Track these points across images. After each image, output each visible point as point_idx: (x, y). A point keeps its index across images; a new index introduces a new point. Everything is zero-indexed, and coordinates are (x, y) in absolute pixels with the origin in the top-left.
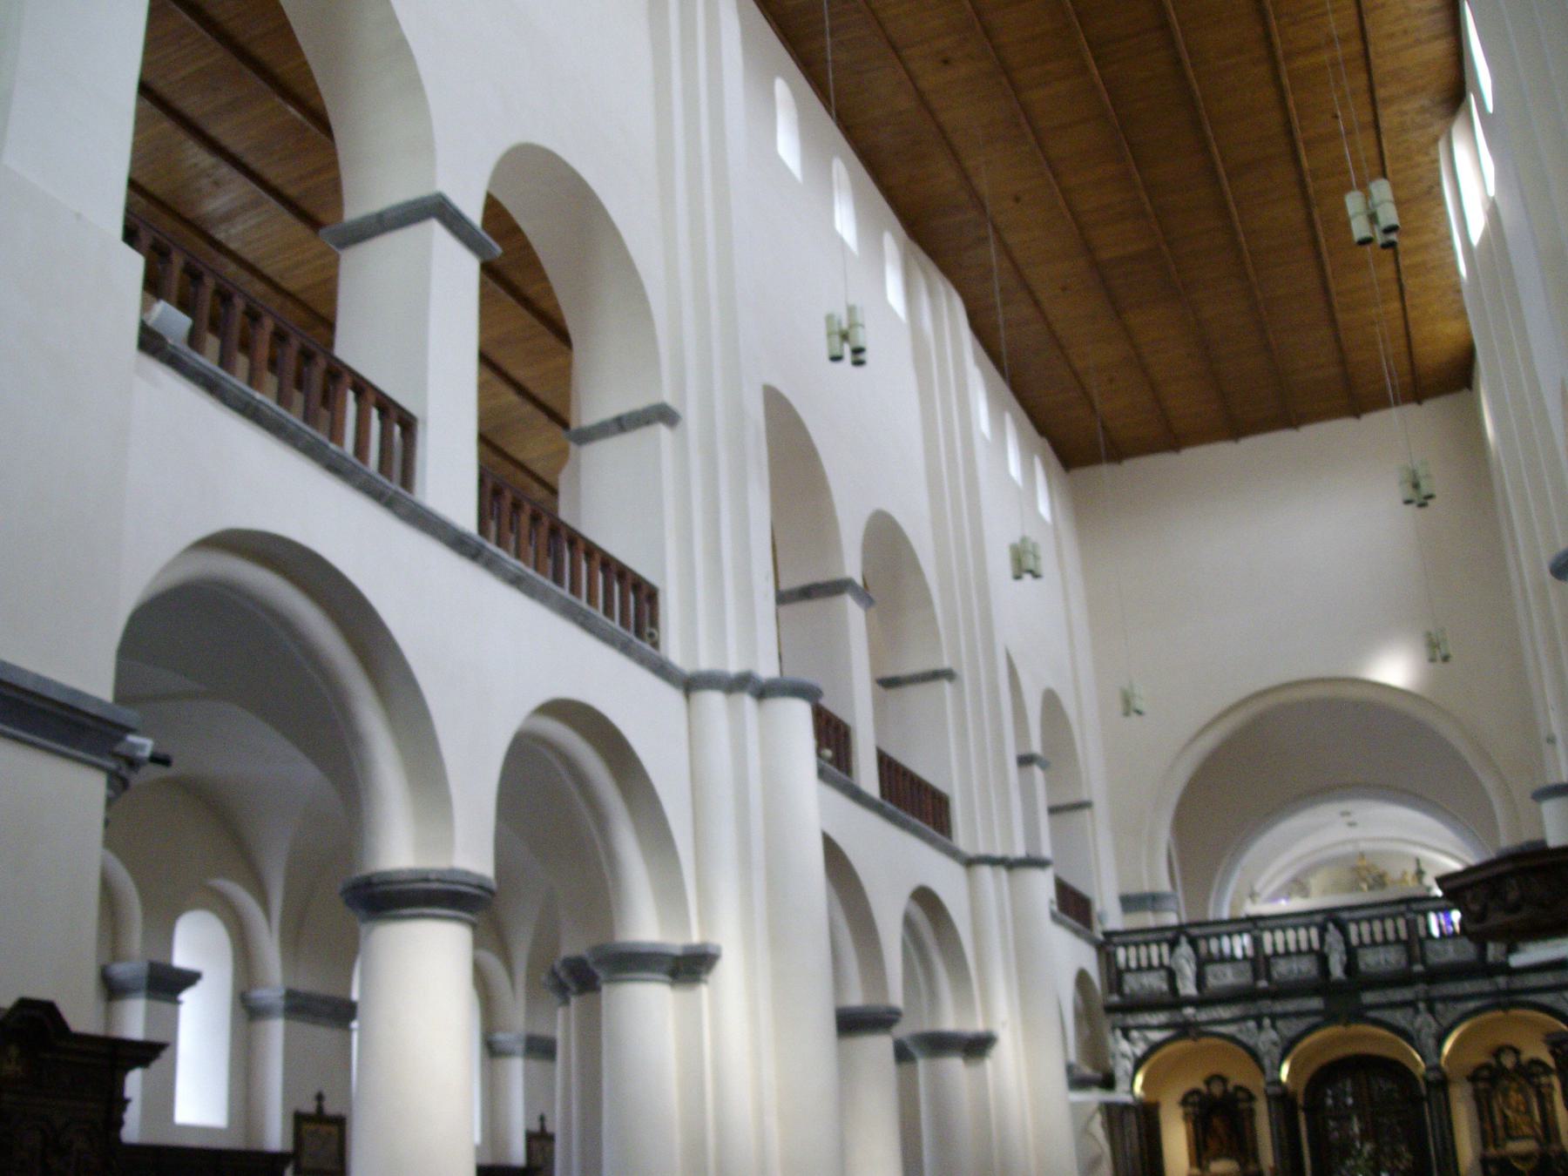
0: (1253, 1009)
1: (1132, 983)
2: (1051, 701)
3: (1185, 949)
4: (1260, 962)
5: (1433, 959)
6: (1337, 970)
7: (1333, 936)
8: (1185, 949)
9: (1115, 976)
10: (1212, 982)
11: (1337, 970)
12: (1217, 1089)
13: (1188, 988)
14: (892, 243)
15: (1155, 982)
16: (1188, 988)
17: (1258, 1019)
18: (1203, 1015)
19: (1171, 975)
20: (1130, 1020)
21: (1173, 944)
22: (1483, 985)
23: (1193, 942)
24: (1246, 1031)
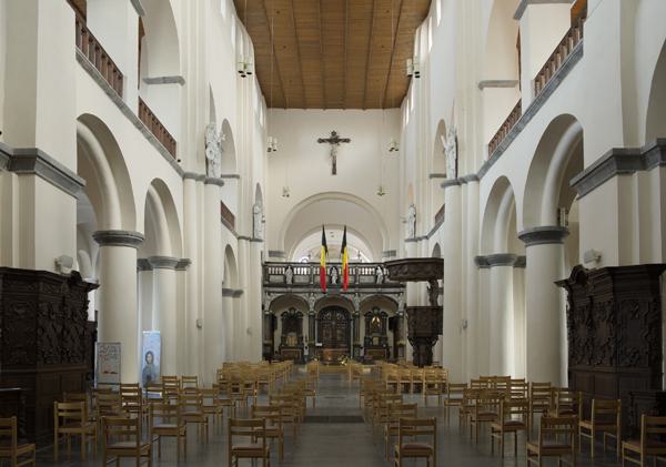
0: (307, 290)
1: (272, 278)
2: (258, 185)
3: (289, 270)
4: (311, 276)
5: (362, 281)
6: (334, 282)
7: (334, 271)
8: (289, 270)
9: (266, 275)
10: (297, 281)
11: (334, 282)
12: (292, 312)
13: (289, 282)
14: (234, 17)
15: (279, 279)
16: (289, 282)
17: (310, 293)
18: (294, 290)
19: (285, 278)
20: (271, 289)
21: (287, 268)
22: (374, 290)
23: (292, 269)
24: (304, 297)
